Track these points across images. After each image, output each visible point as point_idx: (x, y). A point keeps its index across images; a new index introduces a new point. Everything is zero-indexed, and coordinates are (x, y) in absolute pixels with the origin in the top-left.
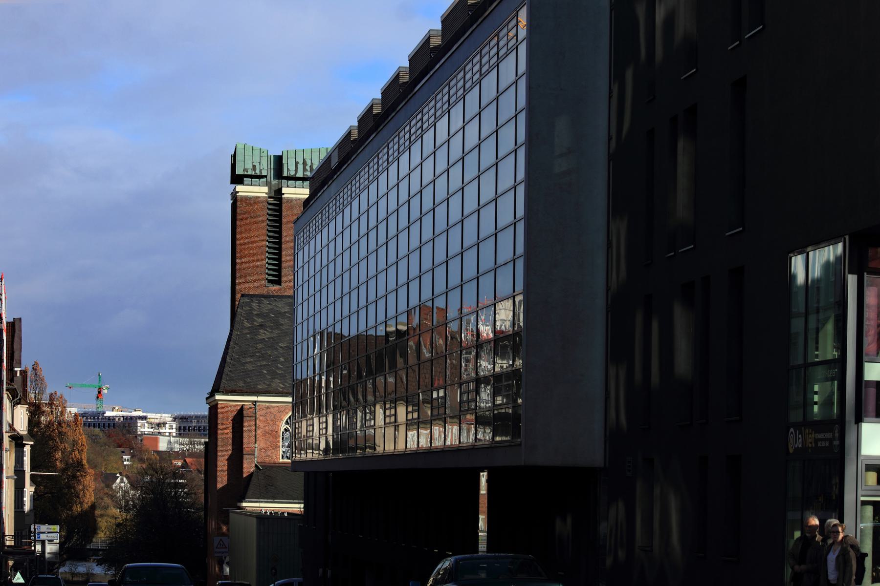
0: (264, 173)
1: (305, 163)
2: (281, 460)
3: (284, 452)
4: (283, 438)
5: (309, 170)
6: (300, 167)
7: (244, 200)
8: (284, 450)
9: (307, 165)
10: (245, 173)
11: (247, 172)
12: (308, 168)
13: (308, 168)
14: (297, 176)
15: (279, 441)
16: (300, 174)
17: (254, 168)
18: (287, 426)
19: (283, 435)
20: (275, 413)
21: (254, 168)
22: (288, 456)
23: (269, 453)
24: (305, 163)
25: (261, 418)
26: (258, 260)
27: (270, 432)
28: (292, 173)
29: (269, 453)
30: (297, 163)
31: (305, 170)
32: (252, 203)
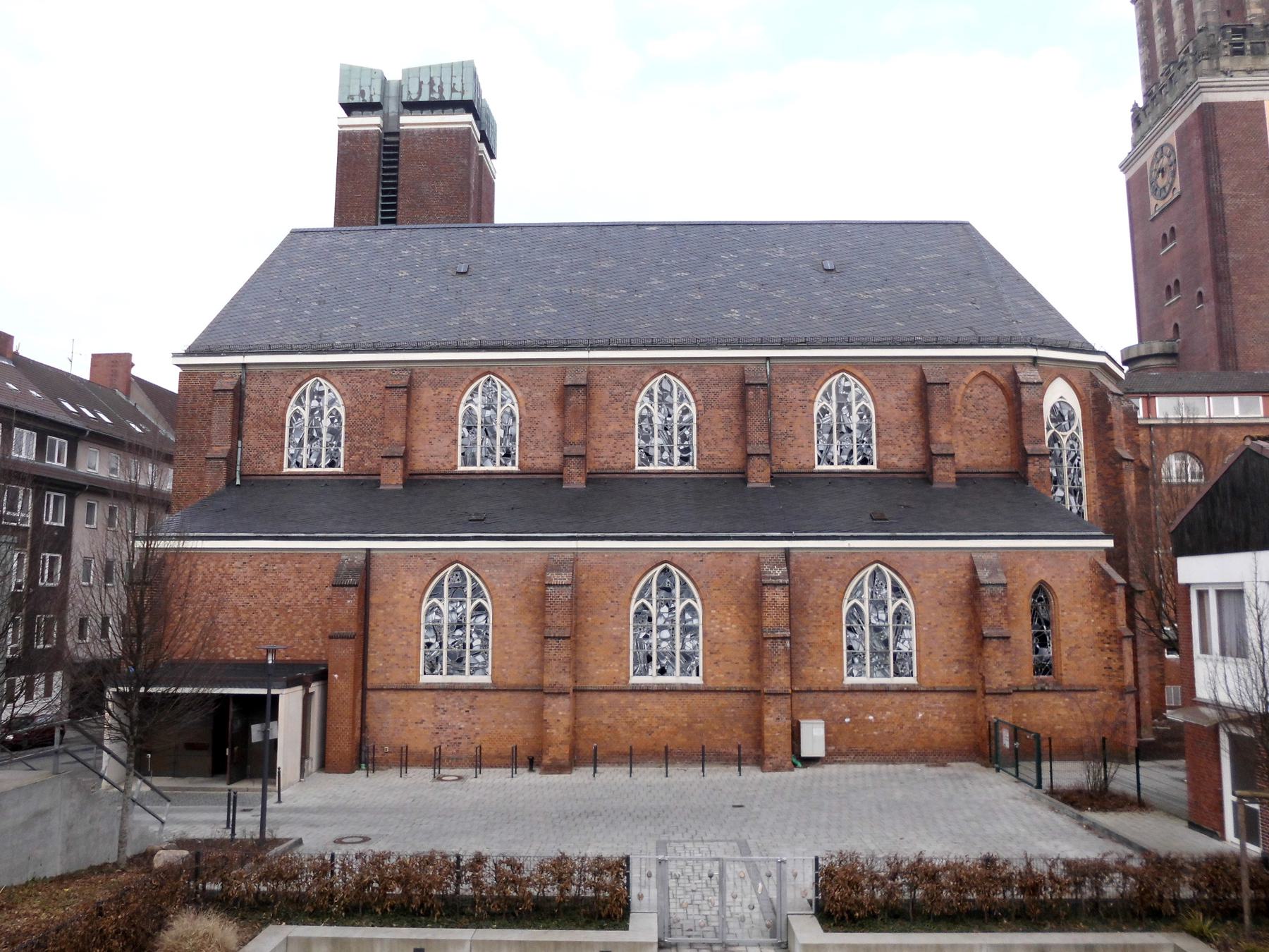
0: (376, 99)
1: (432, 83)
2: (286, 470)
3: (292, 455)
4: (291, 430)
5: (437, 90)
6: (426, 88)
7: (347, 136)
8: (292, 451)
9: (434, 85)
10: (351, 101)
11: (353, 99)
12: (436, 88)
13: (436, 88)
14: (420, 100)
15: (283, 436)
16: (425, 97)
17: (362, 93)
18: (299, 407)
19: (291, 425)
20: (276, 386)
21: (362, 93)
22: (299, 461)
23: (264, 457)
24: (432, 83)
25: (252, 395)
26: (363, 215)
27: (268, 419)
28: (414, 97)
29: (264, 457)
30: (421, 83)
31: (432, 91)
32: (358, 139)
